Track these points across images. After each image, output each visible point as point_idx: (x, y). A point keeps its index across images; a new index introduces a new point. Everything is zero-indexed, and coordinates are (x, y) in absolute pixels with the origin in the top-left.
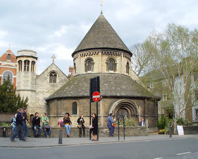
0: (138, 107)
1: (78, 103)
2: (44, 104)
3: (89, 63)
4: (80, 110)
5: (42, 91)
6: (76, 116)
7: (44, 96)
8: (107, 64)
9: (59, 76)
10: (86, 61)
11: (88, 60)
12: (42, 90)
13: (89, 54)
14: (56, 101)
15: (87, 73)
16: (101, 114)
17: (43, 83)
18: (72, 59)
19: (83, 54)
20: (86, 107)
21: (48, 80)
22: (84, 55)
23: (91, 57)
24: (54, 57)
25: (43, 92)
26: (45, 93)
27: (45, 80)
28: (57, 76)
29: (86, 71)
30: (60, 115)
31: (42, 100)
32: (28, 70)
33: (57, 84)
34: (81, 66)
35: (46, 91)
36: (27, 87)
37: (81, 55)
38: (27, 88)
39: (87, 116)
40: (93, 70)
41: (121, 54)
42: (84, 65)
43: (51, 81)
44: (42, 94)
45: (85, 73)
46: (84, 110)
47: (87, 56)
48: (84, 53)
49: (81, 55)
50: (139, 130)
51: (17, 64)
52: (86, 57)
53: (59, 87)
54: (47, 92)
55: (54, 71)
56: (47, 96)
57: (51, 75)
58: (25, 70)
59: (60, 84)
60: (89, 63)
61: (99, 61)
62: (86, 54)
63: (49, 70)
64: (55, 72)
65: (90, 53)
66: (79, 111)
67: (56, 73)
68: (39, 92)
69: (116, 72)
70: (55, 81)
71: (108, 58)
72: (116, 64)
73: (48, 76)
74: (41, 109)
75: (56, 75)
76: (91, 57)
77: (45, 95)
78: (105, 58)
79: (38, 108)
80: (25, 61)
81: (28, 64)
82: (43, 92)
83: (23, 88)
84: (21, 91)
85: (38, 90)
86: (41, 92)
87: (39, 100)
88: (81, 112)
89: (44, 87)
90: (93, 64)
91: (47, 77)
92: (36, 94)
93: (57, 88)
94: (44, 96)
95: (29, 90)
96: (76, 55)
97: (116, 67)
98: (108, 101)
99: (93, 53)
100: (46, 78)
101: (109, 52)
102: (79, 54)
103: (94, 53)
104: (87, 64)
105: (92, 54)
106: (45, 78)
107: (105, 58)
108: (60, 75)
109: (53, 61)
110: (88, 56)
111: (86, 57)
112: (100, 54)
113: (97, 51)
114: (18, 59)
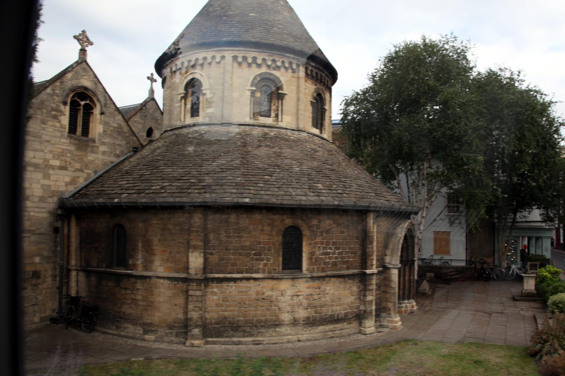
4: (312, 254)
5: (40, 161)
9: (102, 113)
14: (197, 219)
17: (44, 129)
20: (334, 243)
21: (65, 120)
26: (51, 172)
27: (55, 117)
28: (97, 111)
30: (221, 276)
31: (42, 199)
33: (94, 141)
35: (57, 163)
43: (72, 129)
53: (104, 153)
55: (86, 88)
59: (103, 144)
64: (90, 94)
66: (310, 259)
67: (92, 100)
73: (65, 103)
75: (93, 109)
77: (52, 177)
88: (316, 261)
89: (49, 148)
91: (62, 107)
93: (96, 156)
94: (46, 182)
100: (56, 110)
106: (53, 109)
108: (105, 109)
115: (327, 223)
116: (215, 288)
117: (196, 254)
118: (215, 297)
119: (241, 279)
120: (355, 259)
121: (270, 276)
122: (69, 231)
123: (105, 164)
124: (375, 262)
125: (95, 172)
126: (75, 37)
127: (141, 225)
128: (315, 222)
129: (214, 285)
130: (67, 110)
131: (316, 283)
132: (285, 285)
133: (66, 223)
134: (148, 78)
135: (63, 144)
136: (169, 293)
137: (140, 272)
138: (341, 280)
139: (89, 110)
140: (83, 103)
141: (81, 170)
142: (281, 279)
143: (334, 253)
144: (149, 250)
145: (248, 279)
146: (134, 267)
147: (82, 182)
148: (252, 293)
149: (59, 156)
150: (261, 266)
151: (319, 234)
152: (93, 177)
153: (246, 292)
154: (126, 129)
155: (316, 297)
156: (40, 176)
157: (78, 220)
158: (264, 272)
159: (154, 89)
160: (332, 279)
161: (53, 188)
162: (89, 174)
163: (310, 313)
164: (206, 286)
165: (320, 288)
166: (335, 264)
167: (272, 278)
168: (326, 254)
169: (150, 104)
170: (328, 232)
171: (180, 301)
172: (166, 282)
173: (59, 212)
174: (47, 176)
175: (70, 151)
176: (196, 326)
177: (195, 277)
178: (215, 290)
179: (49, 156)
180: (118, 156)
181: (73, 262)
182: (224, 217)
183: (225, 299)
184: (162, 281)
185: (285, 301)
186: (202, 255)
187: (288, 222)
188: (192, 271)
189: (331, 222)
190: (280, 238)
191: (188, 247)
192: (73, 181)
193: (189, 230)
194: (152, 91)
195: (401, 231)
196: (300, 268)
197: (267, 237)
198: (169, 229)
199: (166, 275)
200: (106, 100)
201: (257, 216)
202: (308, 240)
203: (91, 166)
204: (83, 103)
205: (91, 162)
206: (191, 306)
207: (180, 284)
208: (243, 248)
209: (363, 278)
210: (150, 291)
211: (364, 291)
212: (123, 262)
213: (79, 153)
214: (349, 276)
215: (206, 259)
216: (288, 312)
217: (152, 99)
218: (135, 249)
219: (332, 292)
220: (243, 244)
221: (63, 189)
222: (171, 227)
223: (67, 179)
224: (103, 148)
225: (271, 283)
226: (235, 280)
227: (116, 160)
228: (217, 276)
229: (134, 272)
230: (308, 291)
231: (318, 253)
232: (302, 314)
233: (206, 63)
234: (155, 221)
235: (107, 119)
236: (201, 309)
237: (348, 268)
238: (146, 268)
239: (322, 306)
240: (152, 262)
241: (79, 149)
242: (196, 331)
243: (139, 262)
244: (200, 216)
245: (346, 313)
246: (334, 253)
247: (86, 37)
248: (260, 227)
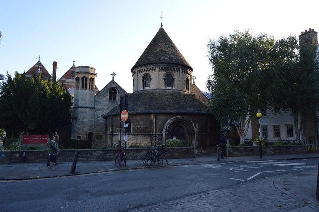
0: (195, 126)
9: (119, 93)
10: (143, 77)
12: (100, 107)
18: (132, 74)
19: (140, 70)
21: (108, 97)
24: (113, 74)
25: (102, 110)
28: (117, 93)
32: (86, 87)
34: (139, 82)
35: (106, 108)
36: (85, 105)
38: (84, 106)
39: (142, 135)
41: (179, 69)
43: (110, 99)
45: (142, 89)
50: (185, 151)
51: (74, 80)
52: (143, 73)
56: (106, 112)
57: (111, 93)
58: (83, 87)
60: (146, 78)
69: (175, 88)
70: (115, 99)
72: (174, 80)
73: (107, 92)
78: (163, 73)
80: (83, 78)
81: (86, 81)
83: (80, 106)
84: (79, 108)
85: (97, 107)
86: (100, 109)
90: (150, 79)
95: (86, 108)
102: (137, 70)
104: (145, 80)
107: (163, 73)
110: (145, 72)
111: (143, 73)
112: (157, 69)
114: (76, 76)
128: (134, 118)
139: (115, 93)
156: (101, 112)
174: (103, 112)
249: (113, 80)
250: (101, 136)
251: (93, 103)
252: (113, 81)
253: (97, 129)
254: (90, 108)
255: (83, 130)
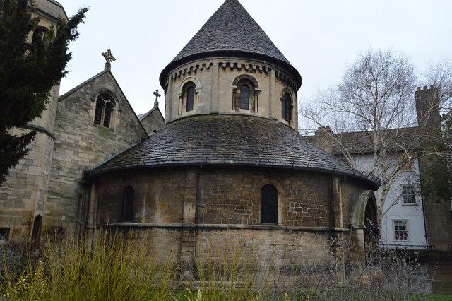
1: (280, 190)
2: (72, 183)
3: (246, 88)
4: (286, 209)
5: (73, 142)
6: (273, 226)
7: (76, 158)
8: (282, 102)
9: (120, 110)
11: (241, 80)
12: (71, 139)
13: (247, 67)
14: (191, 177)
15: (237, 113)
16: (342, 225)
19: (228, 64)
20: (305, 202)
21: (92, 112)
22: (232, 66)
23: (253, 75)
24: (108, 56)
25: (75, 147)
26: (80, 150)
27: (86, 110)
28: (116, 108)
29: (235, 107)
30: (210, 225)
31: (71, 171)
35: (84, 144)
37: (224, 65)
40: (254, 108)
42: (231, 91)
43: (97, 121)
44: (71, 152)
45: (232, 111)
46: (298, 210)
47: (239, 70)
48: (232, 62)
49: (224, 65)
52: (236, 74)
53: (120, 140)
54: (88, 149)
55: (109, 91)
59: (120, 133)
61: (270, 89)
62: (239, 66)
63: (98, 86)
65: (251, 66)
67: (112, 100)
68: (64, 144)
70: (107, 123)
71: (284, 90)
74: (62, 200)
76: (253, 75)
79: (54, 194)
82: (75, 147)
86: (69, 145)
87: (59, 168)
90: (257, 93)
92: (55, 149)
94: (76, 158)
96: (204, 62)
97: (291, 114)
98: (349, 190)
99: (258, 67)
100: (86, 104)
101: (287, 76)
102: (216, 62)
103: (261, 69)
104: (239, 92)
105: (255, 68)
106: (84, 104)
108: (122, 107)
109: (108, 65)
110: (243, 72)
111: (236, 74)
112: (273, 72)
113: (267, 67)
115: (298, 184)
116: (203, 236)
117: (190, 206)
118: (204, 244)
119: (226, 228)
120: (326, 219)
121: (251, 226)
122: (90, 197)
123: (120, 149)
124: (341, 221)
125: (113, 154)
126: (102, 54)
127: (146, 185)
128: (288, 182)
129: (204, 233)
130: (95, 104)
131: (290, 236)
132: (263, 235)
133: (88, 191)
134: (154, 93)
135: (90, 130)
136: (165, 240)
137: (143, 223)
138: (312, 234)
139: (110, 108)
140: (106, 102)
141: (102, 151)
142: (260, 229)
143: (305, 210)
144: (151, 205)
145: (232, 228)
146: (139, 220)
147: (102, 161)
148: (236, 242)
149: (86, 139)
150: (243, 218)
151: (291, 192)
152: (111, 157)
153: (230, 239)
154: (137, 124)
155: (291, 248)
156: (71, 152)
157: (97, 188)
158: (245, 223)
159: (159, 101)
160: (304, 233)
161: (80, 163)
162: (107, 155)
163: (286, 262)
164: (197, 234)
165: (294, 240)
166: (307, 220)
167: (253, 229)
168: (298, 210)
169: (155, 112)
170: (299, 191)
171: (175, 247)
172: (164, 231)
173: (84, 181)
175: (95, 137)
176: (188, 269)
177: (188, 226)
178: (205, 237)
179: (79, 138)
180: (131, 144)
181: (91, 222)
182: (213, 176)
183: (213, 245)
184: (161, 230)
185: (264, 250)
186: (194, 207)
187: (265, 181)
188: (186, 220)
189: (302, 183)
190: (259, 194)
191: (183, 200)
192: (95, 160)
193: (184, 187)
194: (157, 103)
195: (364, 197)
196: (276, 221)
197: (247, 193)
198: (168, 187)
199: (164, 225)
200: (123, 100)
201: (240, 176)
202: (283, 197)
203: (109, 149)
204: (106, 102)
205: (110, 146)
206: (183, 251)
207: (176, 233)
208: (228, 202)
209: (333, 234)
210: (150, 239)
211: (334, 248)
212: (130, 217)
213: (100, 138)
214: (319, 232)
215: (196, 209)
216: (267, 260)
217: (156, 108)
218: (140, 205)
219: (304, 245)
220: (228, 198)
221: (87, 164)
222: (170, 185)
223: (91, 157)
224: (118, 137)
225: (251, 233)
226: (221, 229)
227: (128, 146)
228: (206, 225)
229: (139, 224)
230: (284, 243)
231: (291, 209)
232: (279, 262)
233: (198, 70)
234: (158, 184)
235: (123, 115)
236: (192, 253)
237: (318, 225)
238: (148, 220)
239: (295, 257)
240: (153, 214)
241: (102, 134)
242: (187, 273)
243: (143, 215)
244: (194, 175)
245: (317, 266)
246: (305, 210)
247: (111, 54)
248: (242, 185)
249: (107, 74)
250: (61, 230)
251: (54, 118)
252: (107, 74)
253: (54, 204)
254: (48, 134)
255: (19, 204)
